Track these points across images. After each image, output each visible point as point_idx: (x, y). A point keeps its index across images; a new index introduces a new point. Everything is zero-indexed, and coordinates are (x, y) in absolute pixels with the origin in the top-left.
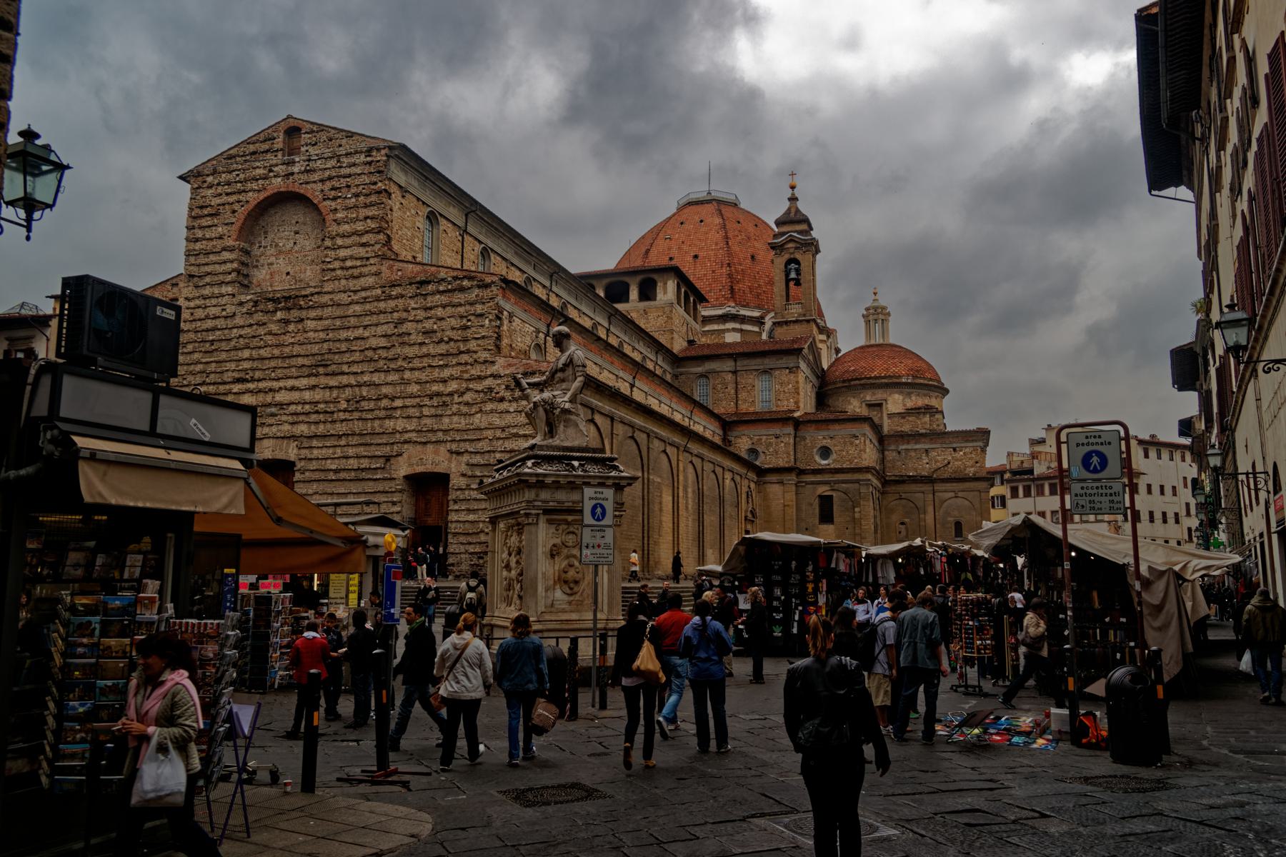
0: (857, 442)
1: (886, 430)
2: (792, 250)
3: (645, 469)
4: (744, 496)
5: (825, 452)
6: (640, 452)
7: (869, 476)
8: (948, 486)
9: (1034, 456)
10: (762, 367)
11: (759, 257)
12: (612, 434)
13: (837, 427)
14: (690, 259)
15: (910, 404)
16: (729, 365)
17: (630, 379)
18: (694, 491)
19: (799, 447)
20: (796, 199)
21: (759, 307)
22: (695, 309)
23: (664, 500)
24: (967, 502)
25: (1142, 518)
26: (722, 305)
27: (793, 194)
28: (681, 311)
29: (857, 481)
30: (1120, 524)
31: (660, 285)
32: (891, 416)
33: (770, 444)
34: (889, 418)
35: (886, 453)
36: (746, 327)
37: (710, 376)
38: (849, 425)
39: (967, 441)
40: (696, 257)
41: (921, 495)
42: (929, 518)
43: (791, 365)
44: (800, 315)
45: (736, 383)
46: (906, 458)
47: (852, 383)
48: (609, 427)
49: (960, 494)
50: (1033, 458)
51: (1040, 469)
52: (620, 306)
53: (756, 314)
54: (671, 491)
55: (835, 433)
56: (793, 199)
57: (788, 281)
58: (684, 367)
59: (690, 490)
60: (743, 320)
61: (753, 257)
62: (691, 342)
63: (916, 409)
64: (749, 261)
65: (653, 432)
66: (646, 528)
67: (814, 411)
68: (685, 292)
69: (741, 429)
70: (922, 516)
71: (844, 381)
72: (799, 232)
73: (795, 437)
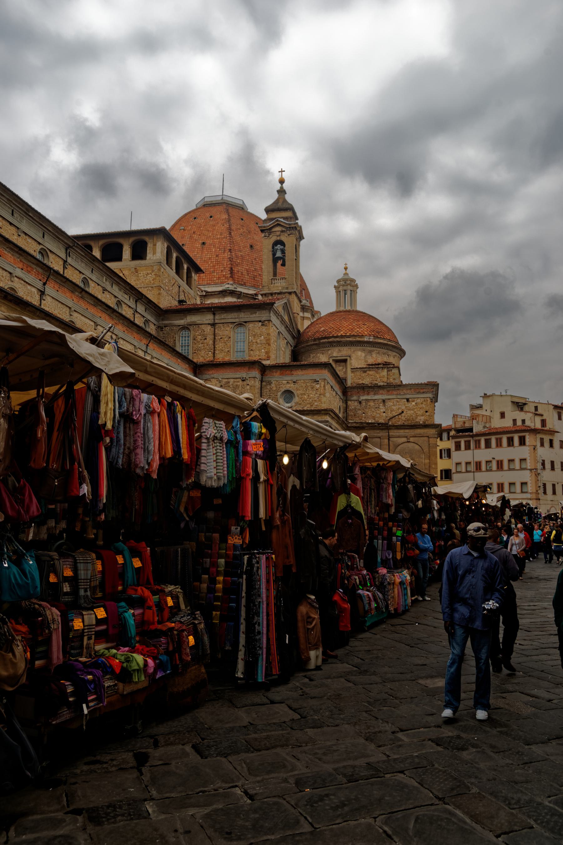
0: (318, 386)
1: (349, 383)
2: (278, 233)
5: (289, 395)
7: (328, 418)
8: (402, 432)
9: (473, 418)
10: (237, 320)
11: (256, 247)
14: (198, 245)
15: (371, 361)
16: (208, 318)
17: (39, 285)
21: (254, 286)
22: (189, 277)
24: (417, 447)
25: (559, 466)
26: (222, 283)
27: (282, 188)
28: (173, 273)
30: (539, 471)
31: (150, 246)
32: (354, 370)
34: (352, 372)
35: (349, 403)
37: (191, 328)
39: (419, 393)
40: (204, 243)
41: (378, 440)
43: (263, 319)
44: (283, 288)
45: (214, 335)
46: (366, 407)
47: (322, 341)
49: (412, 439)
50: (473, 419)
51: (477, 428)
52: (112, 265)
53: (251, 292)
55: (298, 378)
56: (282, 192)
57: (275, 260)
58: (168, 319)
61: (251, 246)
62: (181, 302)
63: (376, 364)
64: (248, 249)
68: (177, 258)
69: (210, 372)
71: (315, 340)
72: (284, 218)
73: (262, 381)
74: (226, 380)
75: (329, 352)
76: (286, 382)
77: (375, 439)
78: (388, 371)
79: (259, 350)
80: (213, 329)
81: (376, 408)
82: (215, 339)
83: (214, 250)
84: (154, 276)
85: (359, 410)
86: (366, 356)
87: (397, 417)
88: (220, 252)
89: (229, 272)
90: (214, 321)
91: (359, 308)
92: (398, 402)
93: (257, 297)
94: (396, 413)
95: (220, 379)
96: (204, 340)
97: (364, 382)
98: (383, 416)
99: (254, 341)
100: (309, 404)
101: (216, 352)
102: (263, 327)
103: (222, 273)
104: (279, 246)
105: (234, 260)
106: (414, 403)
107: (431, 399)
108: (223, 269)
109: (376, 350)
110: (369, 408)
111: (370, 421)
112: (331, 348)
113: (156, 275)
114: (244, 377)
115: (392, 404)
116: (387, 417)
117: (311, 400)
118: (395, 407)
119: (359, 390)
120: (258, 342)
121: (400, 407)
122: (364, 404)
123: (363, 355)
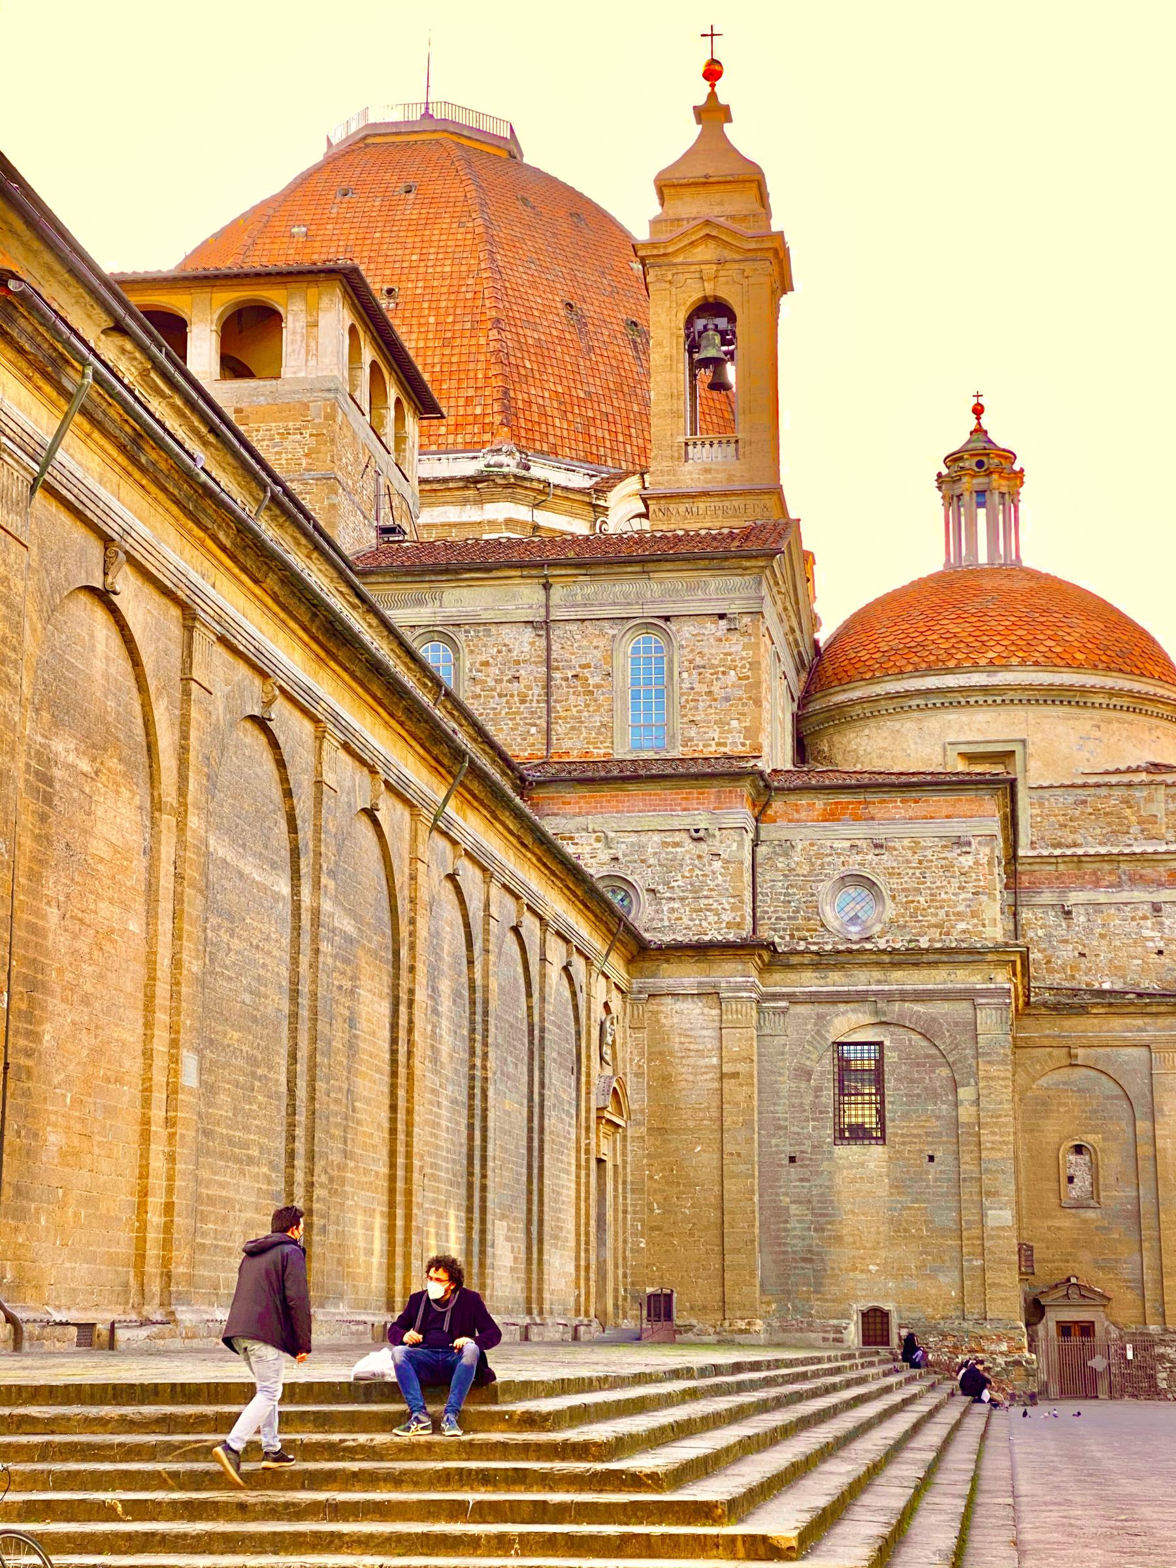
0: (967, 861)
3: (305, 868)
4: (595, 1033)
6: (288, 794)
12: (187, 680)
13: (897, 807)
18: (457, 994)
19: (766, 876)
20: (725, 114)
23: (363, 1010)
26: (472, 448)
29: (969, 995)
33: (671, 865)
35: (1026, 915)
36: (545, 519)
37: (460, 637)
38: (938, 802)
43: (732, 609)
48: (177, 652)
53: (579, 481)
54: (387, 979)
59: (445, 986)
60: (543, 495)
65: (336, 717)
66: (301, 1118)
67: (789, 766)
70: (1143, 1125)
73: (756, 844)
74: (633, 838)
76: (847, 844)
77: (1130, 1050)
79: (720, 723)
80: (543, 643)
82: (549, 678)
83: (432, 320)
84: (312, 441)
85: (1066, 941)
88: (458, 327)
89: (497, 407)
90: (548, 612)
91: (1031, 559)
93: (601, 503)
95: (611, 835)
96: (509, 681)
99: (705, 689)
100: (936, 926)
101: (559, 729)
102: (734, 637)
103: (470, 410)
105: (513, 360)
108: (471, 392)
110: (1102, 936)
111: (1106, 986)
113: (317, 435)
114: (702, 826)
117: (942, 913)
120: (715, 689)
122: (1082, 919)
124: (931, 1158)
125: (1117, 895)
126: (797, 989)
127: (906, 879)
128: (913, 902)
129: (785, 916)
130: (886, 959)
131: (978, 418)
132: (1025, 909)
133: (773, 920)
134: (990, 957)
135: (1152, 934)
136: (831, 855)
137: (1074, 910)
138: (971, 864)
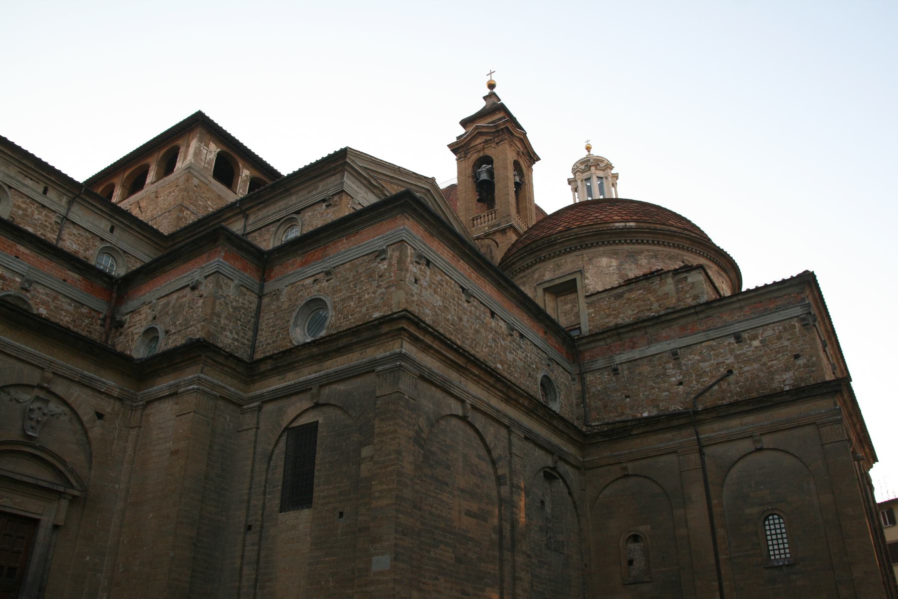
2: (480, 147)
8: (735, 424)
15: (633, 272)
34: (590, 305)
42: (697, 513)
49: (767, 441)
75: (536, 276)
76: (312, 279)
77: (664, 458)
78: (677, 283)
81: (658, 376)
85: (616, 390)
86: (621, 264)
87: (716, 387)
92: (712, 348)
94: (713, 377)
97: (620, 321)
98: (677, 393)
104: (484, 166)
106: (756, 343)
107: (803, 319)
109: (648, 251)
111: (645, 414)
112: (538, 266)
115: (697, 357)
116: (688, 394)
117: (364, 309)
118: (707, 364)
119: (609, 341)
121: (721, 360)
122: (626, 372)
123: (614, 263)
124: (341, 514)
125: (647, 351)
126: (265, 391)
127: (344, 292)
128: (346, 307)
129: (271, 341)
130: (315, 350)
131: (589, 151)
132: (588, 375)
133: (264, 346)
134: (385, 329)
135: (674, 372)
136: (301, 291)
137: (619, 367)
138: (386, 267)
